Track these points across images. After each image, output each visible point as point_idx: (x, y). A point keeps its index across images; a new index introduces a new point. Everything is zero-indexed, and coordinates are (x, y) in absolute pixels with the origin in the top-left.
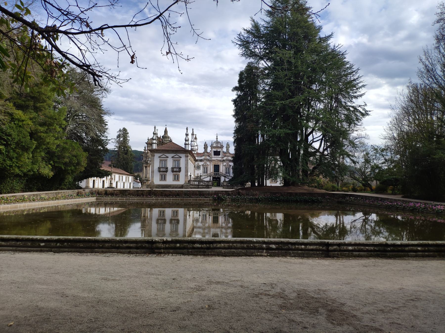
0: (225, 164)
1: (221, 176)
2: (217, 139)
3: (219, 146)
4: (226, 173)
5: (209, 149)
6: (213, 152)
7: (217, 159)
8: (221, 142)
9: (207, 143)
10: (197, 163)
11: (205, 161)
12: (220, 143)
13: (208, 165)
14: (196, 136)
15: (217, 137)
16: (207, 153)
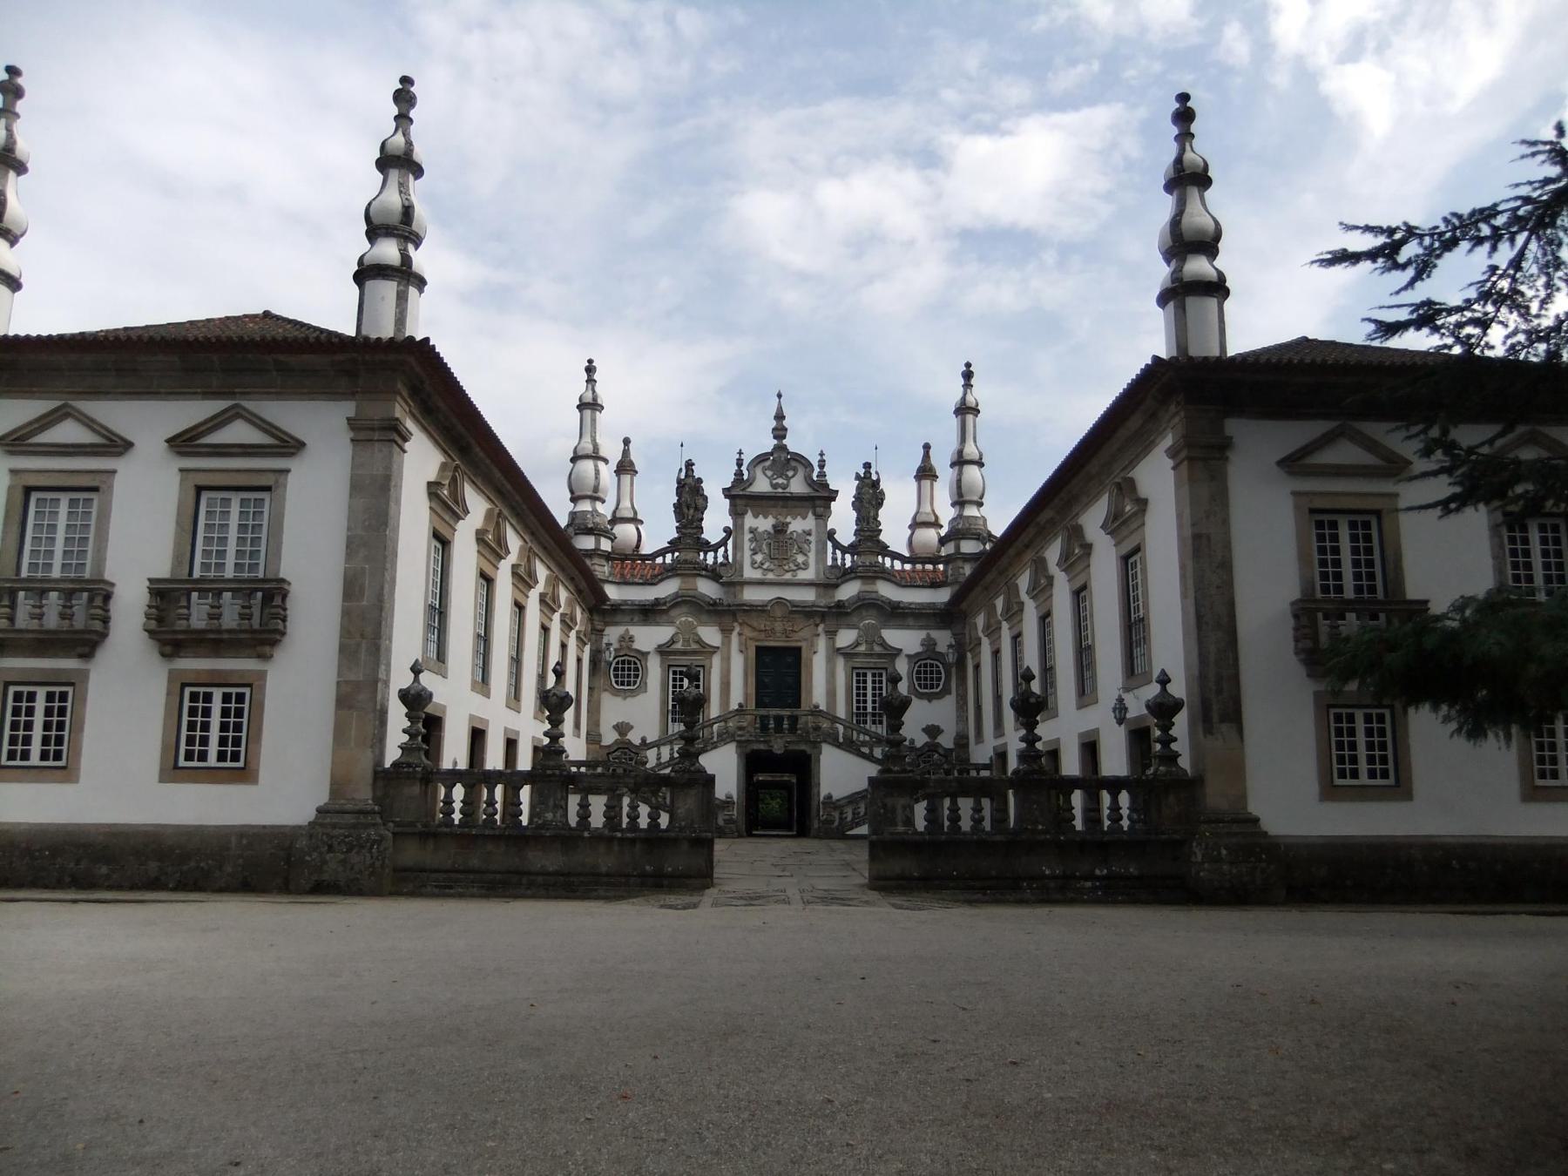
0: (846, 638)
1: (816, 745)
2: (780, 432)
3: (797, 486)
4: (861, 714)
5: (716, 521)
6: (747, 536)
7: (779, 601)
8: (815, 462)
9: (697, 475)
10: (613, 634)
11: (683, 618)
12: (807, 464)
13: (708, 651)
14: (626, 453)
15: (780, 417)
16: (707, 547)
